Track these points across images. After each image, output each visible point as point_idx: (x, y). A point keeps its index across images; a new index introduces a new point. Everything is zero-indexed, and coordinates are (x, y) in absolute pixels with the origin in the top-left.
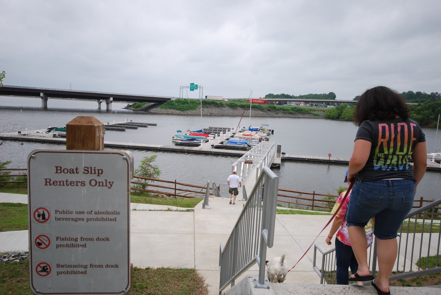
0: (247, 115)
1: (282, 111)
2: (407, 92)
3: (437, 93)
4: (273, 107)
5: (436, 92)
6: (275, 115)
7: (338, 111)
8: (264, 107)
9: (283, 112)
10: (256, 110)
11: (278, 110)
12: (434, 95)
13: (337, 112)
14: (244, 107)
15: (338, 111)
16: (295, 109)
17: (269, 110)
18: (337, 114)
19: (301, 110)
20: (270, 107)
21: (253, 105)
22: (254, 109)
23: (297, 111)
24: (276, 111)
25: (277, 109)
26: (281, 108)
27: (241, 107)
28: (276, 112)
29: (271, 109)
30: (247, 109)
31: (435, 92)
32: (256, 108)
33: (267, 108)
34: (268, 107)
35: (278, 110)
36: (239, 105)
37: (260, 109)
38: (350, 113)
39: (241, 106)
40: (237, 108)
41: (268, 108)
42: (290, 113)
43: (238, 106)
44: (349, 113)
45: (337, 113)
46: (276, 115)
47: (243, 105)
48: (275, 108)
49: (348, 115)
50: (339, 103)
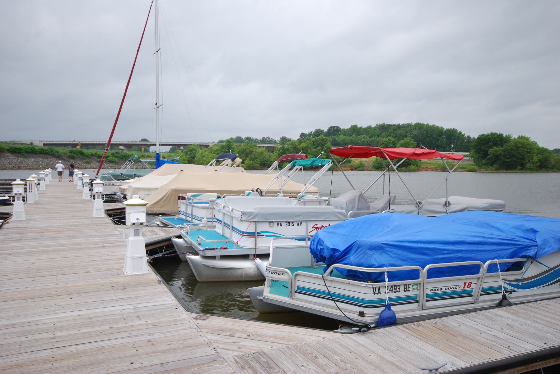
0: (28, 167)
1: (96, 158)
2: (235, 137)
3: (268, 138)
4: (79, 153)
5: (267, 137)
6: (84, 165)
7: (188, 156)
8: (62, 152)
9: (99, 159)
10: (46, 158)
11: (88, 157)
12: (266, 140)
13: (186, 157)
14: (19, 153)
15: (188, 156)
16: (118, 155)
17: (73, 158)
18: (186, 160)
19: (129, 155)
20: (71, 152)
21: (39, 149)
22: (41, 155)
23: (122, 158)
24: (85, 159)
25: (87, 155)
26: (94, 154)
27: (13, 152)
28: (86, 160)
29: (75, 155)
30: (27, 156)
31: (266, 137)
32: (46, 154)
33: (66, 154)
34: (69, 152)
35: (88, 157)
36: (7, 148)
37: (55, 157)
38: (209, 158)
39: (11, 150)
40: (4, 153)
41: (69, 154)
42: (113, 162)
43: (5, 151)
44: (207, 158)
45: (186, 159)
46: (87, 166)
47: (17, 149)
48: (82, 154)
49: (207, 161)
50: (176, 148)
